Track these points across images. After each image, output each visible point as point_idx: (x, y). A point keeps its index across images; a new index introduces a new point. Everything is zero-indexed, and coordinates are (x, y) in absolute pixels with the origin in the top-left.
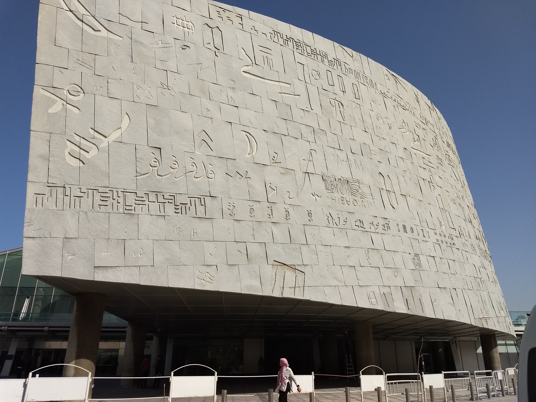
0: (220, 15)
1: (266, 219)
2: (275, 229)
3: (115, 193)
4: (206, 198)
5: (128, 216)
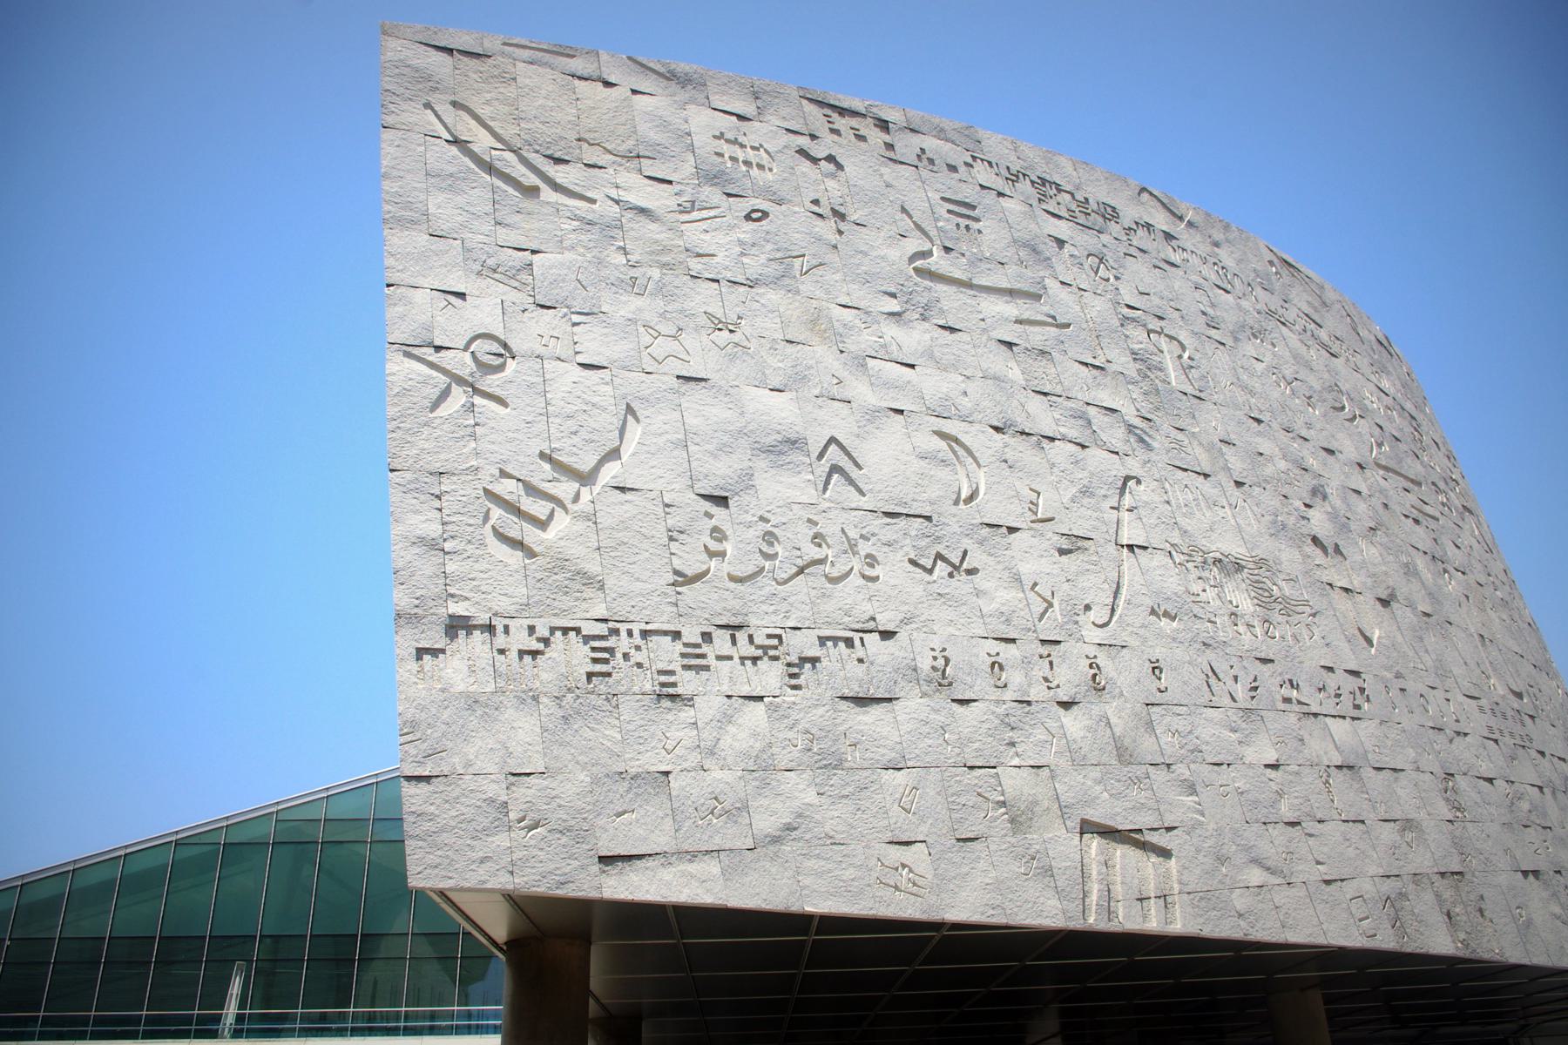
2: (1073, 723)
3: (624, 634)
4: (866, 636)
5: (666, 703)
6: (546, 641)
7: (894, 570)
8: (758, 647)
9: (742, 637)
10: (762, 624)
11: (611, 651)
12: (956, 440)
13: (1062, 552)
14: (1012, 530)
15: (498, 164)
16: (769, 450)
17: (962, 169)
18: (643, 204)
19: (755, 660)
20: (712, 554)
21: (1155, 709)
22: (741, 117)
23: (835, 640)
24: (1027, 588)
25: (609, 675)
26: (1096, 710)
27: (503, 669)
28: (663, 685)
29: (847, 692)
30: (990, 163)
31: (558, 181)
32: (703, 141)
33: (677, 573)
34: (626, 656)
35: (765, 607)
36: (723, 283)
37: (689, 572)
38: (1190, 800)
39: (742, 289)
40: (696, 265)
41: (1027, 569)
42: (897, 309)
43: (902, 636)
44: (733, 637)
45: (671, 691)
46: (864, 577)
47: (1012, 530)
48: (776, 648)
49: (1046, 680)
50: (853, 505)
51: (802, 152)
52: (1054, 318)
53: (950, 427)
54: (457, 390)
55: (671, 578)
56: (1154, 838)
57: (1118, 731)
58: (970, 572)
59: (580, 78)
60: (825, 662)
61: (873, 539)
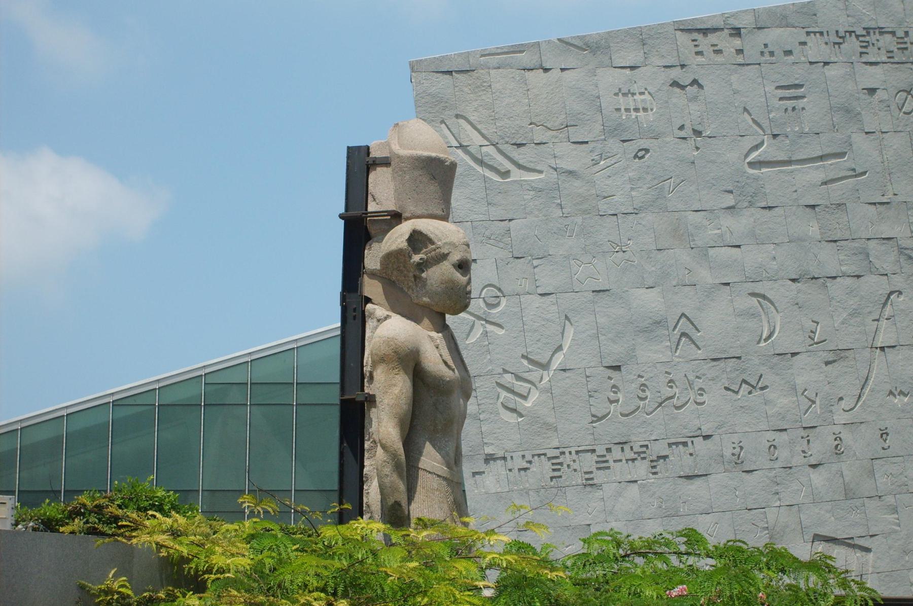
0: (697, 49)
1: (798, 460)
2: (817, 478)
3: (567, 454)
5: (588, 489)
6: (530, 462)
7: (715, 398)
8: (635, 453)
9: (627, 448)
10: (638, 441)
11: (561, 464)
12: (764, 297)
13: (827, 363)
14: (794, 354)
15: (486, 159)
16: (645, 331)
17: (797, 49)
18: (570, 168)
19: (633, 460)
20: (611, 402)
21: (877, 461)
22: (632, 68)
23: (677, 444)
24: (799, 394)
25: (561, 477)
26: (835, 467)
27: (512, 479)
28: (587, 479)
29: (682, 473)
30: (821, 33)
31: (521, 162)
32: (608, 102)
33: (593, 416)
34: (568, 466)
35: (639, 430)
36: (620, 216)
37: (600, 415)
38: (892, 517)
39: (631, 217)
40: (603, 206)
41: (800, 381)
42: (732, 203)
43: (716, 438)
44: (622, 448)
45: (591, 482)
46: (696, 402)
47: (794, 354)
48: (644, 452)
49: (804, 452)
50: (693, 358)
51: (675, 84)
52: (854, 170)
53: (759, 288)
54: (478, 323)
55: (590, 419)
56: (861, 542)
57: (847, 479)
58: (762, 389)
59: (529, 70)
60: (671, 458)
61: (703, 378)
